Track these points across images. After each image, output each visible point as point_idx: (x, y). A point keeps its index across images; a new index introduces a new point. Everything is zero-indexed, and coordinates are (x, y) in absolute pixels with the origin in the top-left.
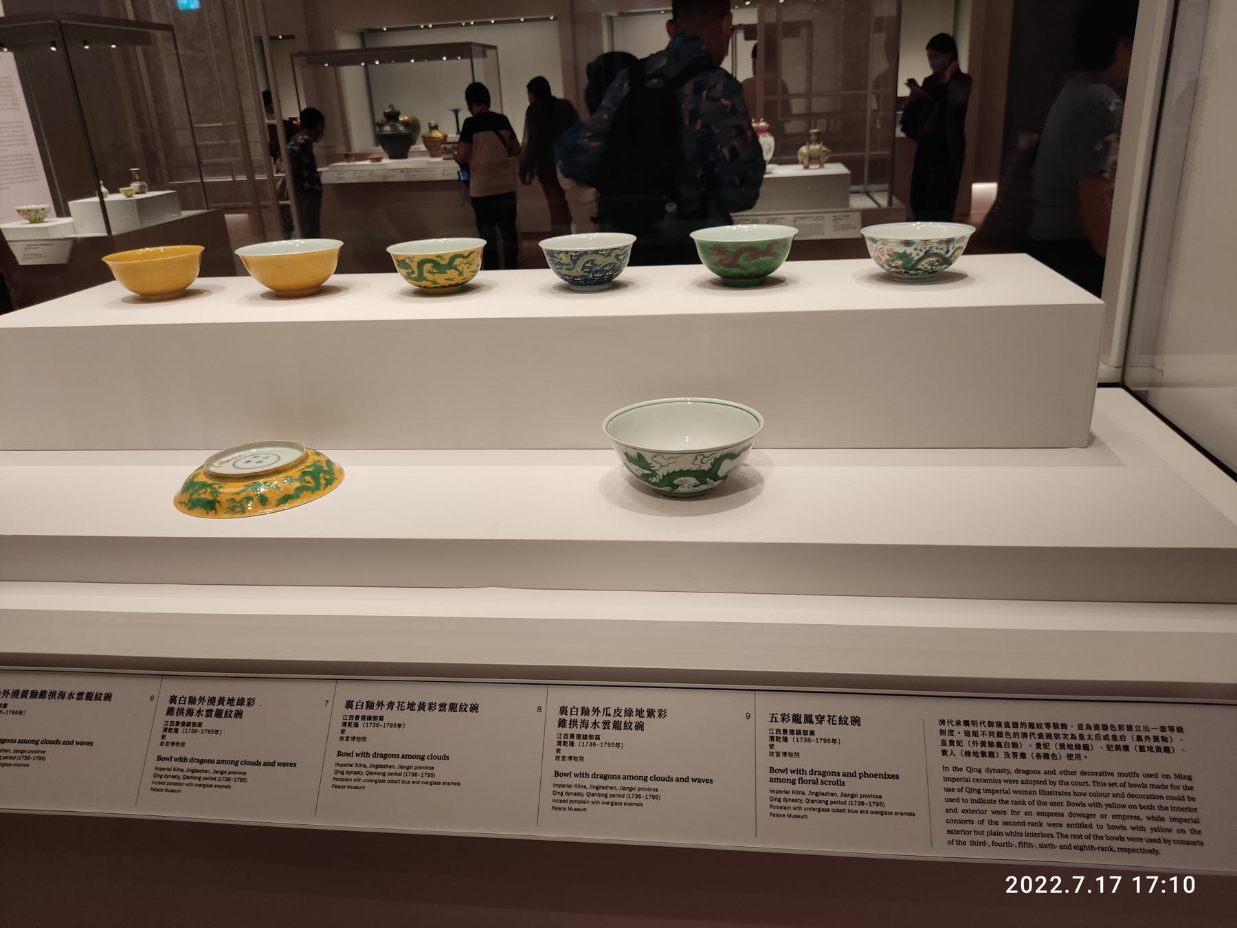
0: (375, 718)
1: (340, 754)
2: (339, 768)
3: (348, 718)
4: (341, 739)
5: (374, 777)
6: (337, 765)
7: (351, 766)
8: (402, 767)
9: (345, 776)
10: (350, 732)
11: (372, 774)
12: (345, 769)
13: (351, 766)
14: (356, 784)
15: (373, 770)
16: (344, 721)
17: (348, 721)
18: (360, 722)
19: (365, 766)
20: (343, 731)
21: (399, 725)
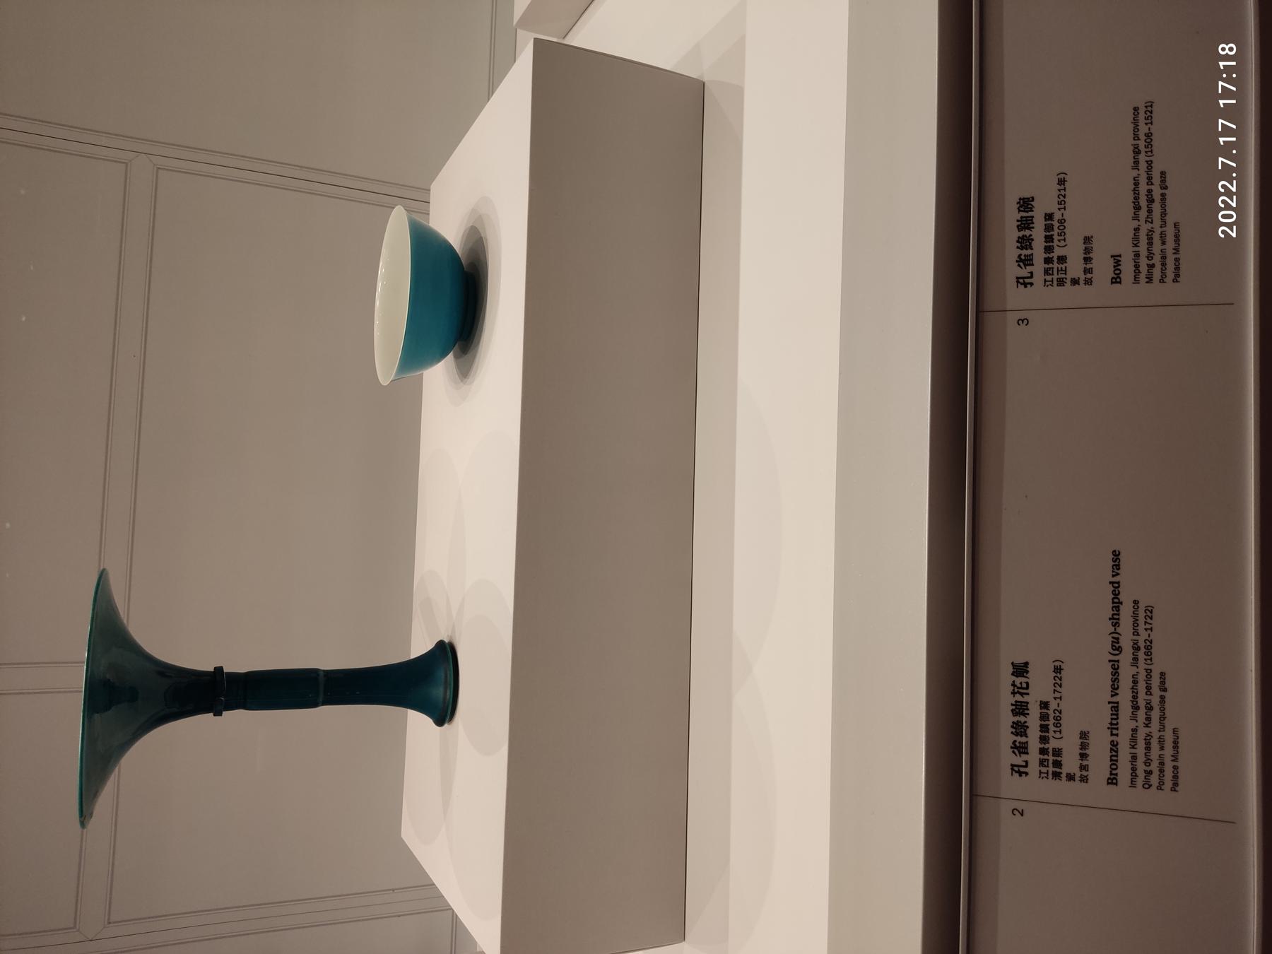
0: (1044, 717)
1: (1112, 781)
3: (1044, 770)
4: (1084, 779)
5: (1155, 714)
7: (1134, 758)
8: (1136, 659)
9: (1154, 766)
10: (1071, 763)
11: (1149, 719)
12: (1141, 768)
13: (1134, 758)
15: (1141, 714)
16: (1050, 776)
17: (1051, 769)
18: (1053, 744)
19: (1135, 730)
20: (1070, 777)
21: (1058, 670)
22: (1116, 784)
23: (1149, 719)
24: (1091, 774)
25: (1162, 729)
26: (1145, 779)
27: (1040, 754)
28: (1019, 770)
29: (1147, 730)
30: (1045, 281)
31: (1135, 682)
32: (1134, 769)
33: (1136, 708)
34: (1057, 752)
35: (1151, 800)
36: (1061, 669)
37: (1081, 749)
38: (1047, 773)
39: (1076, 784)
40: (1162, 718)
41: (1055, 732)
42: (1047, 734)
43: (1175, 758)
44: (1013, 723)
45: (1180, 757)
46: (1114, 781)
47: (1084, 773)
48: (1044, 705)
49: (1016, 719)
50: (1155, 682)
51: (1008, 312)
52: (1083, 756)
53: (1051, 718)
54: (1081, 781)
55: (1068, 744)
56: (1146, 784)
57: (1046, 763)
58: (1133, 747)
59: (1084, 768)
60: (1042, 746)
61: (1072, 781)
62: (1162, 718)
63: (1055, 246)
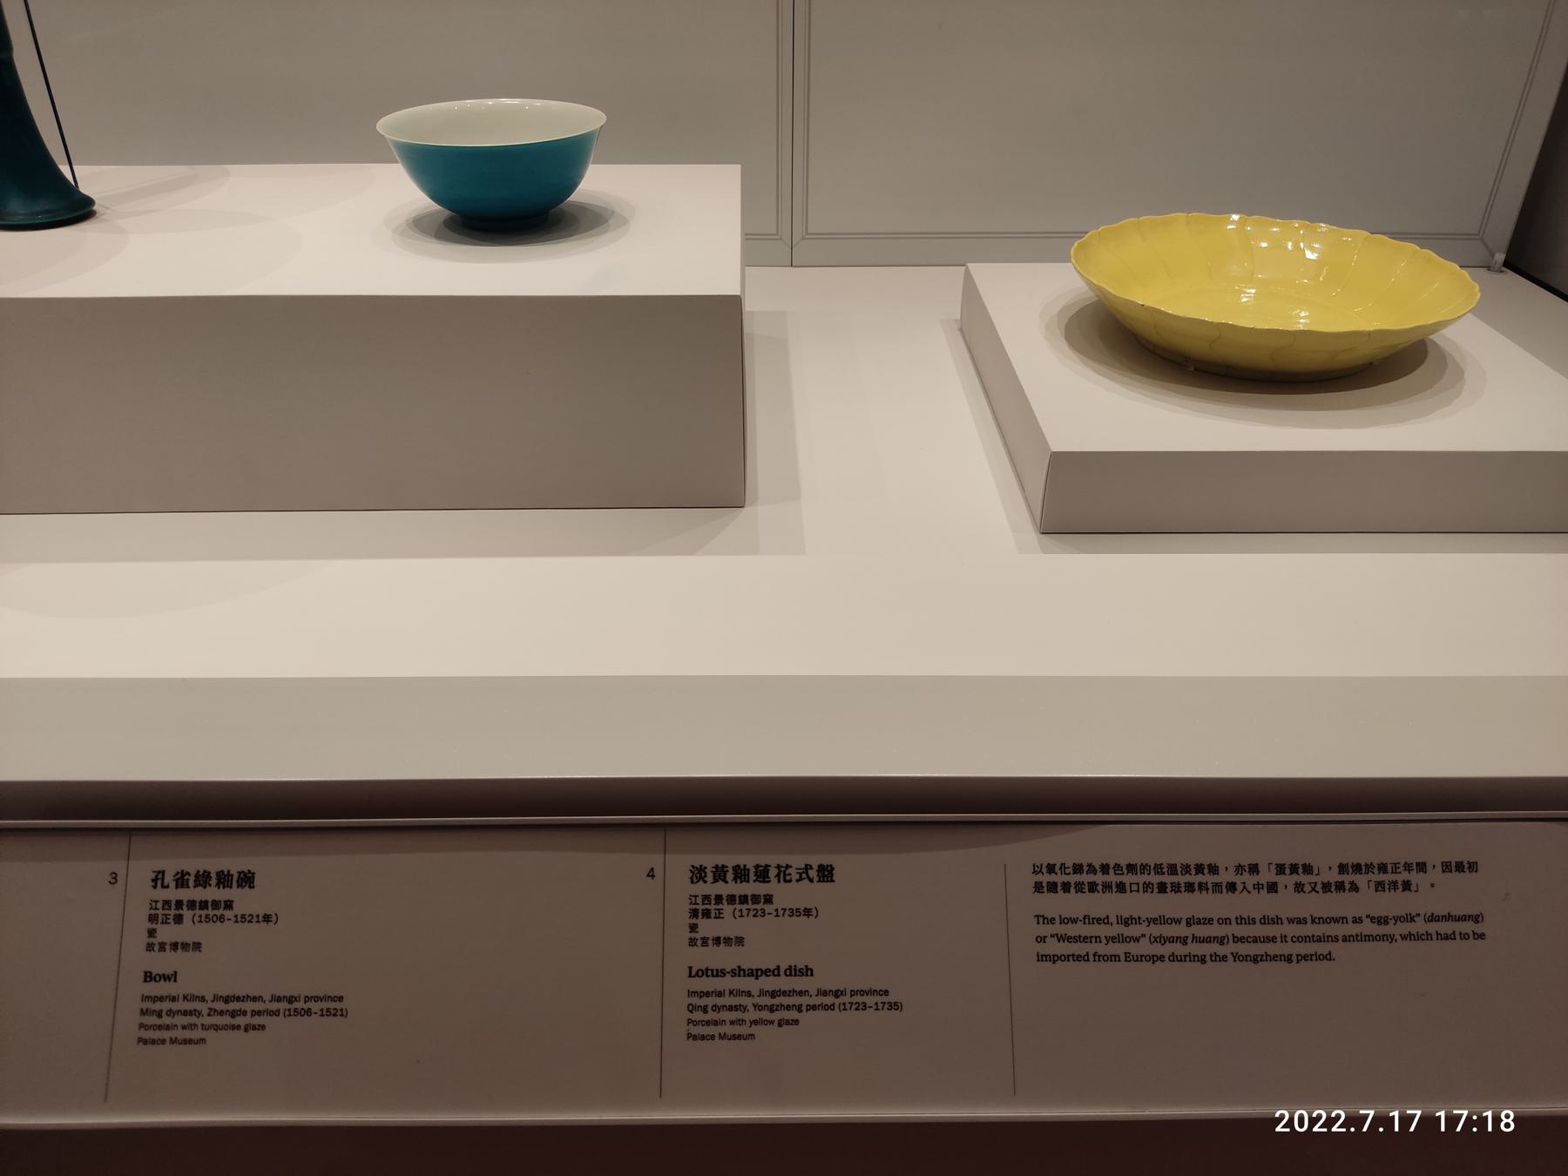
0: (216, 904)
1: (149, 977)
2: (149, 1005)
4: (150, 947)
6: (145, 998)
9: (166, 1020)
10: (167, 933)
12: (166, 1006)
13: (174, 999)
14: (188, 1034)
15: (220, 1006)
16: (153, 912)
17: (160, 912)
18: (187, 914)
19: (203, 999)
20: (152, 933)
22: (145, 981)
23: (221, 1013)
24: (156, 954)
25: (204, 1027)
26: (151, 1008)
27: (177, 901)
28: (158, 879)
29: (205, 1012)
30: (696, 896)
31: (254, 999)
32: (161, 999)
33: (227, 1000)
34: (179, 919)
35: (130, 1018)
36: (268, 921)
37: (182, 944)
38: (156, 909)
39: (145, 939)
40: (216, 1028)
41: (200, 916)
42: (198, 908)
43: (173, 1041)
44: (209, 873)
45: (176, 1047)
46: (148, 979)
47: (156, 948)
48: (229, 905)
49: (213, 875)
50: (257, 1020)
51: (663, 855)
52: (175, 946)
53: (216, 912)
54: (148, 944)
55: (188, 930)
56: (143, 1013)
57: (166, 907)
58: (185, 998)
59: (162, 947)
60: (185, 902)
61: (147, 935)
62: (216, 1028)
63: (735, 906)
